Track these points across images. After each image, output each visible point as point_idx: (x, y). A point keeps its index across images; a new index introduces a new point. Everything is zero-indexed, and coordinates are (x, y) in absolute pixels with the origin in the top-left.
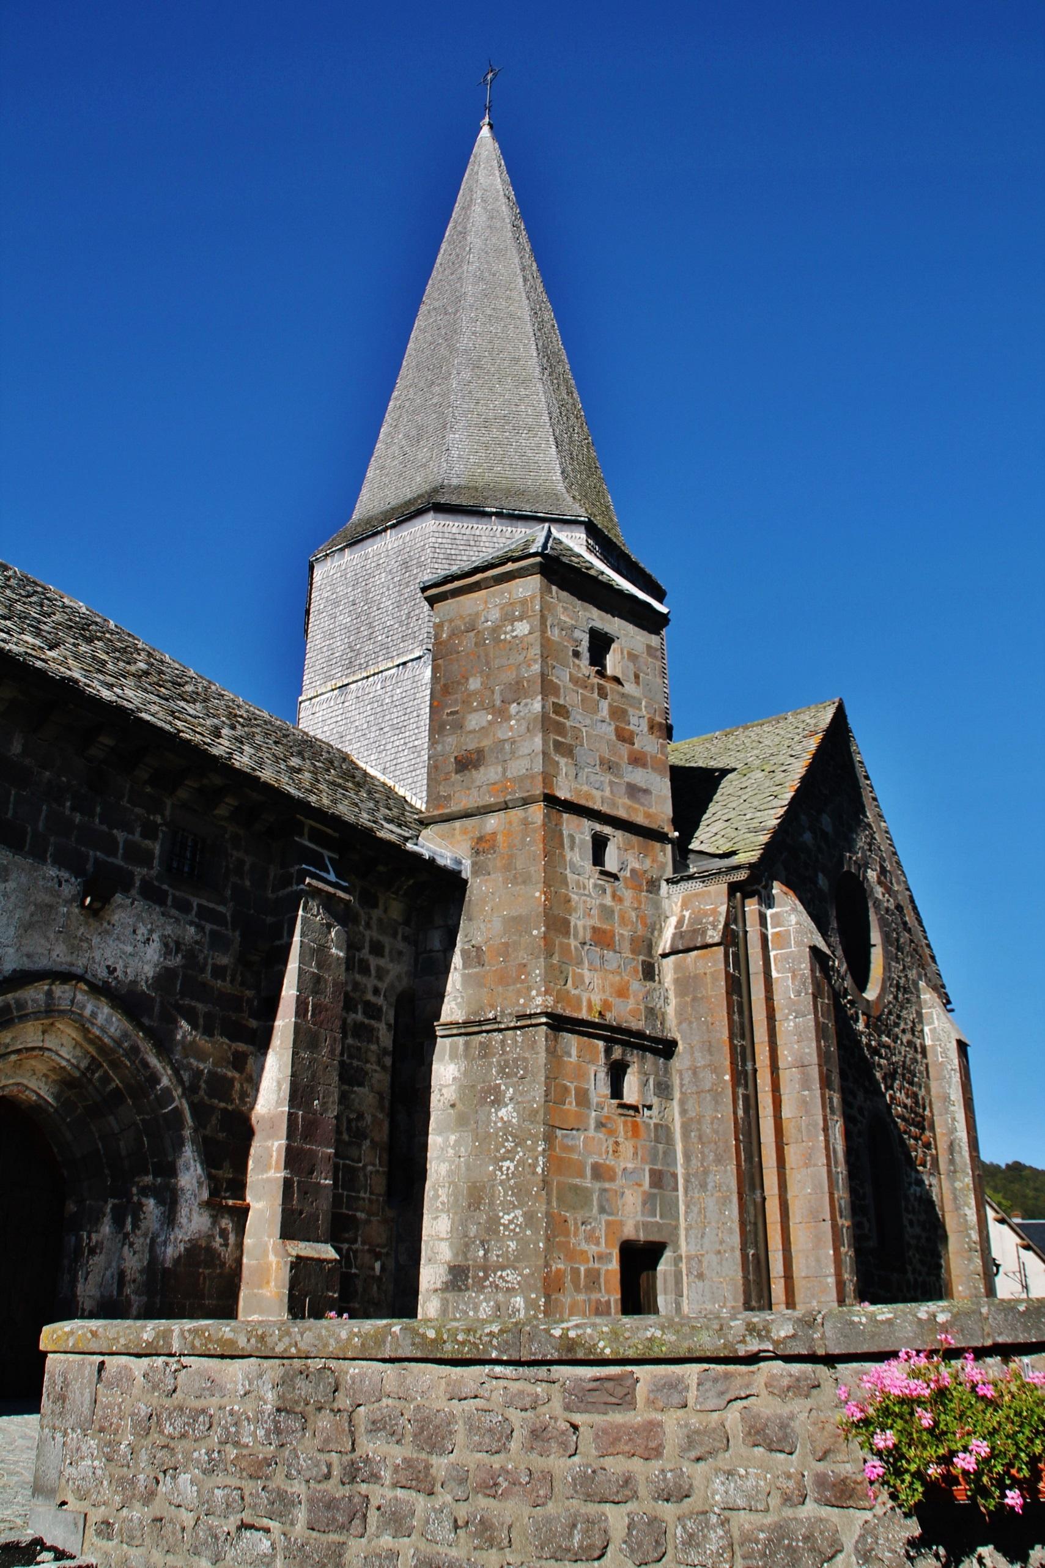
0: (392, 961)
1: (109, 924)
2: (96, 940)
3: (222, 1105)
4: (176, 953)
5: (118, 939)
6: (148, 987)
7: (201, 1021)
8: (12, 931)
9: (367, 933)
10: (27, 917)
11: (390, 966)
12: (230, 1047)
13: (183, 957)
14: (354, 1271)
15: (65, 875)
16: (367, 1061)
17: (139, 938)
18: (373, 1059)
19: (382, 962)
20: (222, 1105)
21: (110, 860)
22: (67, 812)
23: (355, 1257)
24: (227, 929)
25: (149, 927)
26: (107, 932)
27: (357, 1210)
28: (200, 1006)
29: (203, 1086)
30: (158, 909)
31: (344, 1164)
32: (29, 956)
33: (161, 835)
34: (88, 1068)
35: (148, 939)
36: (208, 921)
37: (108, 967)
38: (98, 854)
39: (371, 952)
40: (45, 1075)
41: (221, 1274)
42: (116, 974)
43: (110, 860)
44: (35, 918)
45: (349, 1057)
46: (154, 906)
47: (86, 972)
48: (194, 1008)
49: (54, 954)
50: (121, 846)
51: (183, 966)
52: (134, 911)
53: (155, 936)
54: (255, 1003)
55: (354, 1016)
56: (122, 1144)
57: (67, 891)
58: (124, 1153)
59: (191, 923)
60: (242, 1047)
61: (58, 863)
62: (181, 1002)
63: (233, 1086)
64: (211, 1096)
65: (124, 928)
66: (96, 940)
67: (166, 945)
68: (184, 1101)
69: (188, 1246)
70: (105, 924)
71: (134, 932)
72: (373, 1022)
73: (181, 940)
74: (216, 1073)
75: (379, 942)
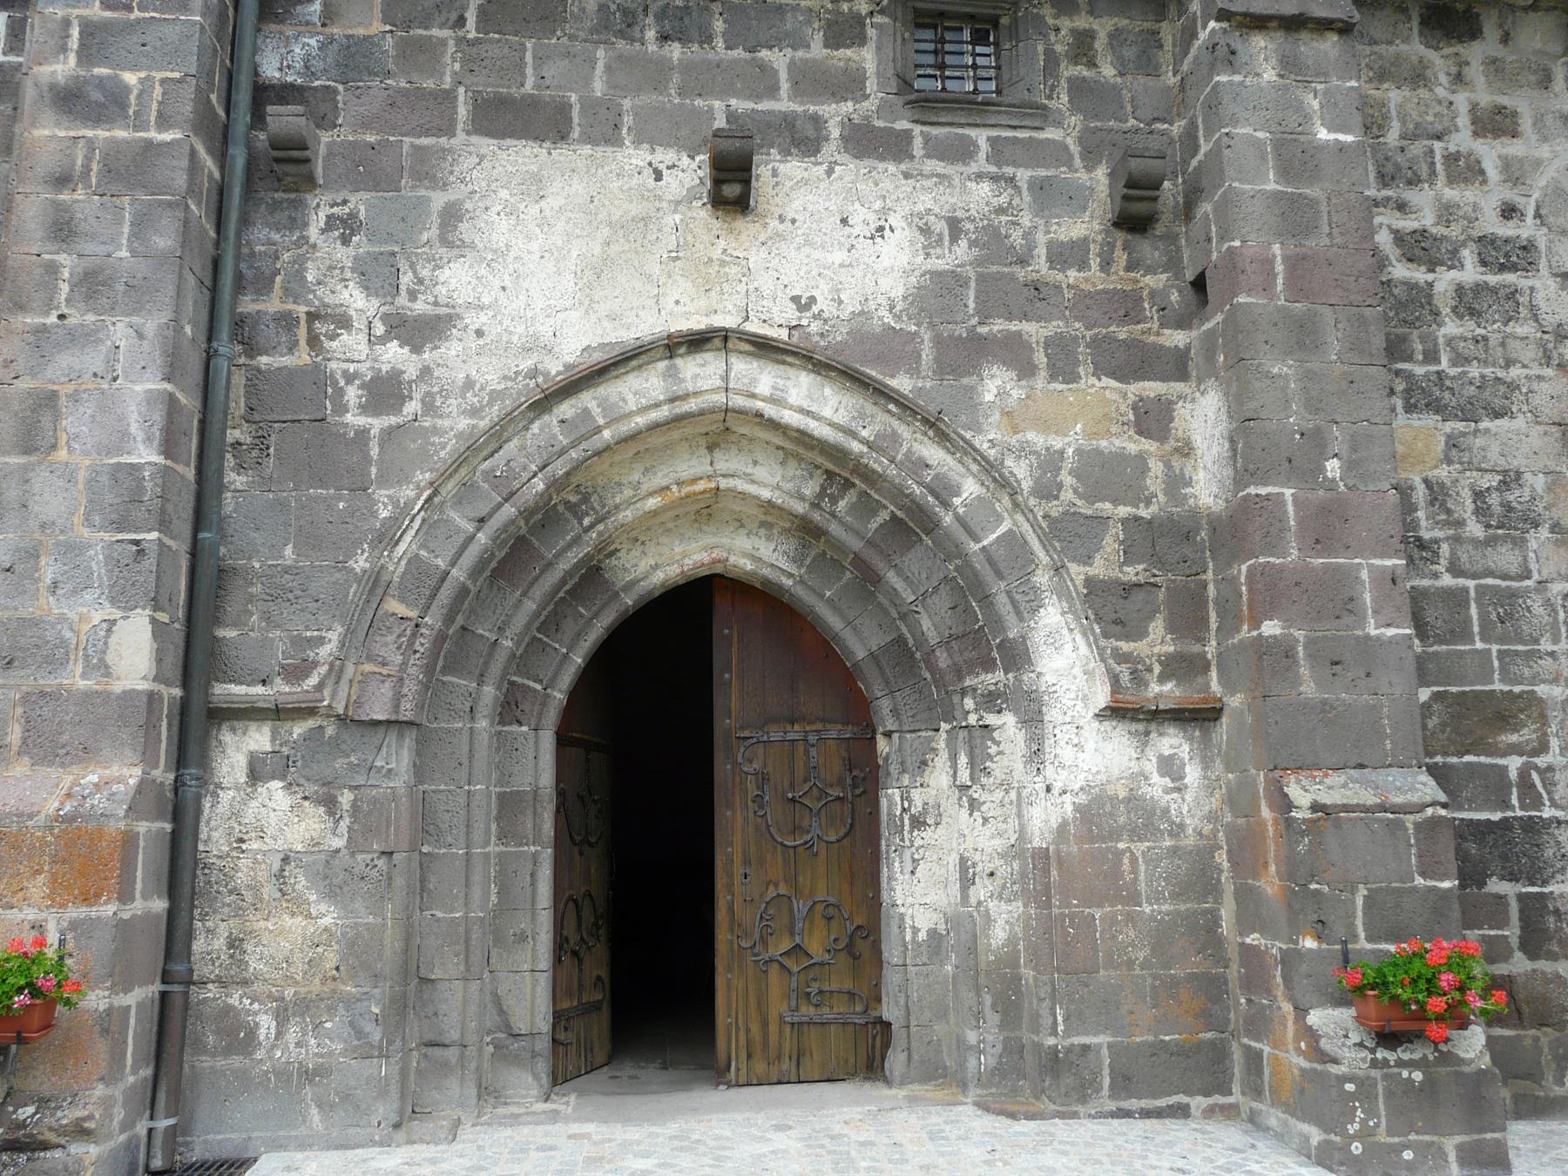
0: (1545, 139)
1: (782, 219)
2: (756, 258)
3: (1124, 511)
4: (954, 239)
5: (807, 242)
6: (898, 317)
7: (1040, 358)
8: (568, 282)
9: (1462, 100)
10: (597, 250)
11: (1544, 151)
12: (1125, 396)
13: (973, 244)
14: (1547, 813)
15: (664, 156)
16: (1509, 363)
17: (856, 231)
18: (1529, 353)
19: (1515, 148)
20: (1124, 511)
21: (765, 105)
22: (652, 48)
23: (1549, 785)
24: (1072, 169)
25: (878, 205)
26: (779, 236)
27: (1535, 679)
28: (1030, 329)
29: (1067, 479)
30: (892, 168)
31: (1478, 587)
32: (612, 318)
33: (871, 33)
34: (821, 494)
35: (881, 229)
36: (1015, 164)
37: (795, 299)
38: (733, 102)
39: (1476, 134)
40: (762, 524)
41: (1174, 851)
42: (815, 309)
43: (765, 105)
44: (615, 248)
45: (1454, 363)
46: (881, 166)
47: (747, 318)
48: (1019, 334)
49: (669, 303)
50: (783, 76)
51: (978, 262)
52: (837, 185)
53: (895, 220)
54: (1174, 297)
55: (1454, 274)
56: (926, 624)
57: (674, 185)
58: (933, 637)
59: (979, 177)
60: (1152, 388)
61: (643, 137)
62: (983, 330)
63: (1145, 470)
64: (1091, 499)
65: (820, 221)
66: (756, 258)
67: (925, 231)
68: (1020, 518)
69: (1083, 799)
70: (774, 224)
71: (844, 221)
72: (1510, 278)
73: (959, 214)
74: (1098, 452)
75: (1500, 110)
